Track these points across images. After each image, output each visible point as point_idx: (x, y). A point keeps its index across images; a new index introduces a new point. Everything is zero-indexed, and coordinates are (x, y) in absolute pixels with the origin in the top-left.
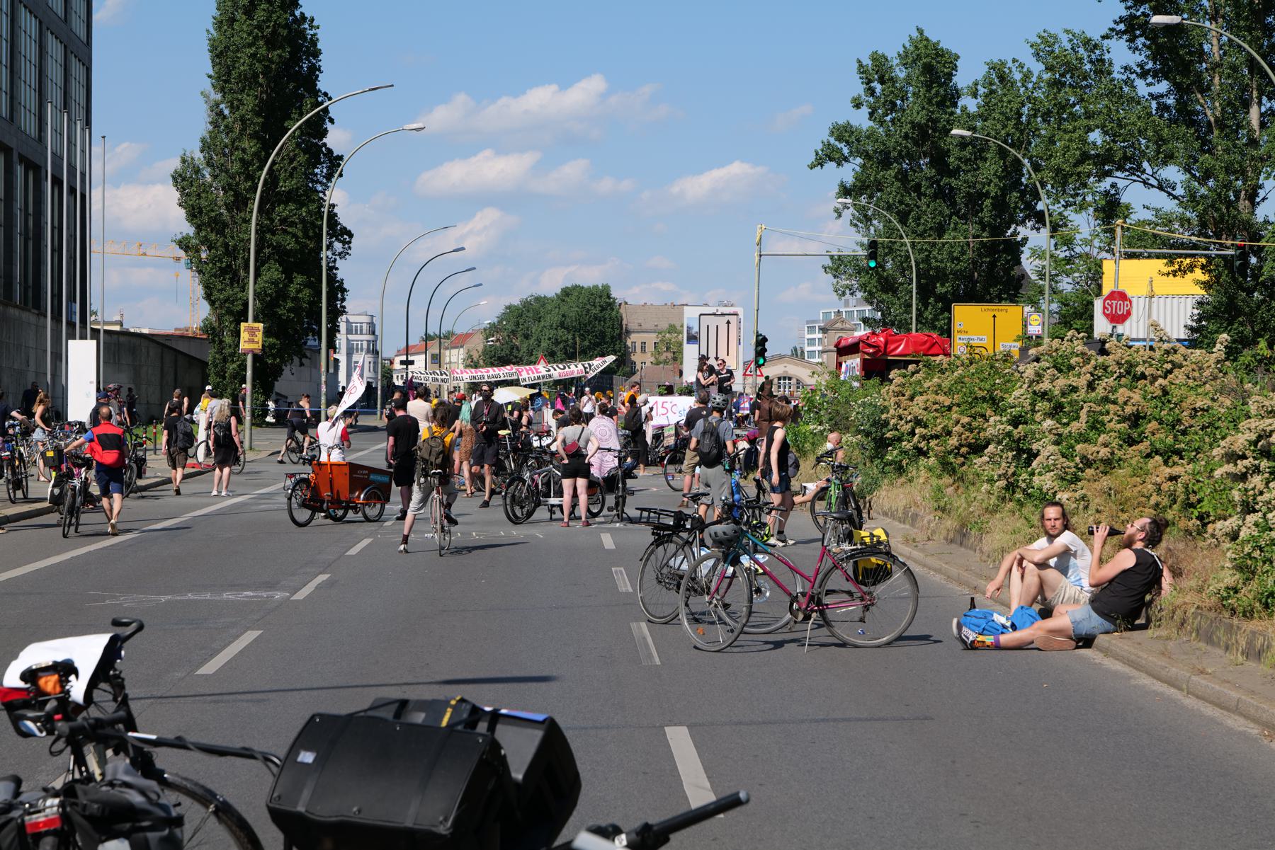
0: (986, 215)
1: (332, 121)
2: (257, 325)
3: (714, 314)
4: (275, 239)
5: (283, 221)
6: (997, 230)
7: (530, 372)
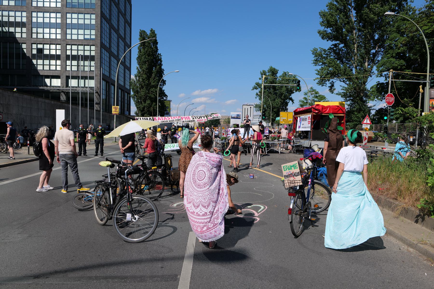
0: (283, 97)
1: (164, 74)
2: (117, 107)
3: (247, 105)
4: (149, 95)
5: (151, 92)
6: (284, 100)
7: (186, 119)
